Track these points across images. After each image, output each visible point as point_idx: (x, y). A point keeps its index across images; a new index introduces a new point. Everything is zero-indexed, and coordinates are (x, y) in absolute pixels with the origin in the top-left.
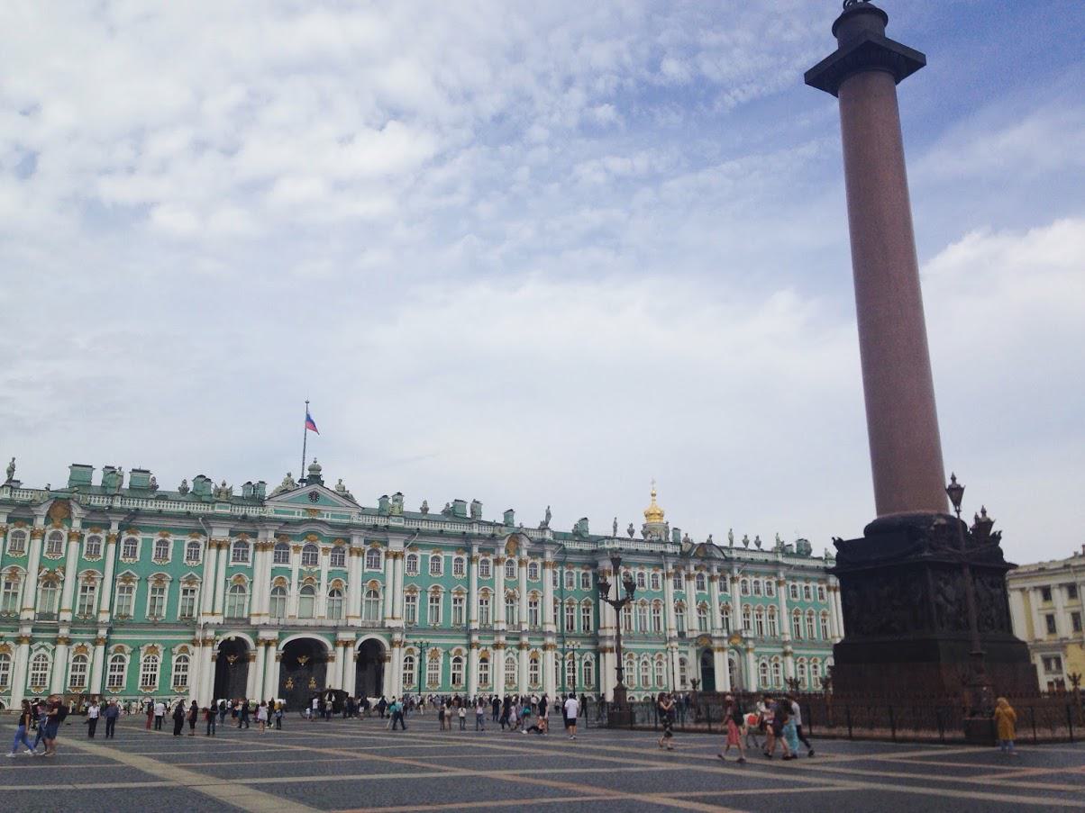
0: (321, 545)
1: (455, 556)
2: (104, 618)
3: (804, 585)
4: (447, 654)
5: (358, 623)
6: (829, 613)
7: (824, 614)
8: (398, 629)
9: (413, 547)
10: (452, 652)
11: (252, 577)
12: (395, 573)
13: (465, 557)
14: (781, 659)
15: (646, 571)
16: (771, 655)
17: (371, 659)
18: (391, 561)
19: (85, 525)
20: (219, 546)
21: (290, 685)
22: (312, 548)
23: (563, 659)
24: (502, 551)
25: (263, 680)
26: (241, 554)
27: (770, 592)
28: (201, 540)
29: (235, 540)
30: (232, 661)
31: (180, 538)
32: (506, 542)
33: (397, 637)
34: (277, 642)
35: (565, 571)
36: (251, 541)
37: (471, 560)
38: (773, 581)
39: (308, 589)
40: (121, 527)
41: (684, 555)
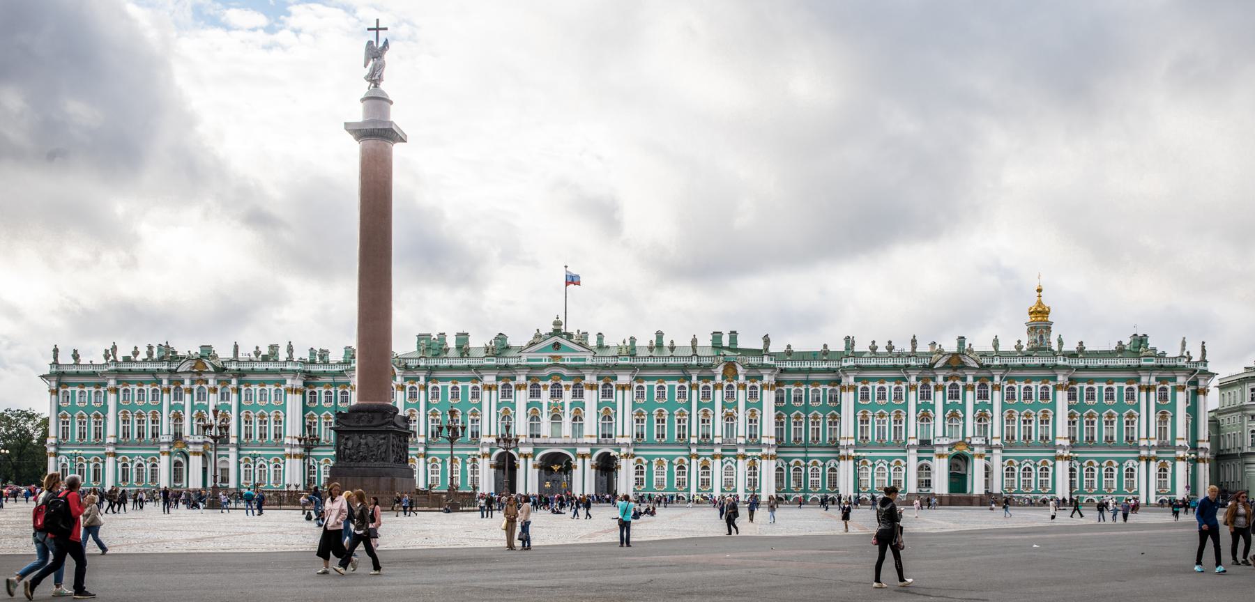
0: (563, 383)
1: (677, 384)
2: (422, 440)
3: (1105, 386)
4: (670, 463)
5: (594, 441)
6: (1136, 414)
7: (1130, 415)
8: (626, 445)
9: (637, 379)
10: (676, 461)
11: (514, 409)
12: (624, 401)
13: (686, 384)
14: (1050, 463)
15: (886, 385)
16: (1036, 459)
17: (607, 466)
18: (620, 392)
19: (406, 379)
20: (490, 388)
21: (548, 485)
22: (556, 385)
23: (806, 467)
24: (719, 378)
25: (528, 480)
26: (507, 392)
27: (1045, 396)
28: (479, 385)
29: (501, 383)
30: (506, 467)
31: (465, 384)
32: (720, 370)
33: (624, 451)
34: (534, 456)
35: (811, 389)
36: (511, 383)
37: (691, 387)
38: (1050, 386)
39: (556, 417)
40: (427, 379)
41: (931, 366)
